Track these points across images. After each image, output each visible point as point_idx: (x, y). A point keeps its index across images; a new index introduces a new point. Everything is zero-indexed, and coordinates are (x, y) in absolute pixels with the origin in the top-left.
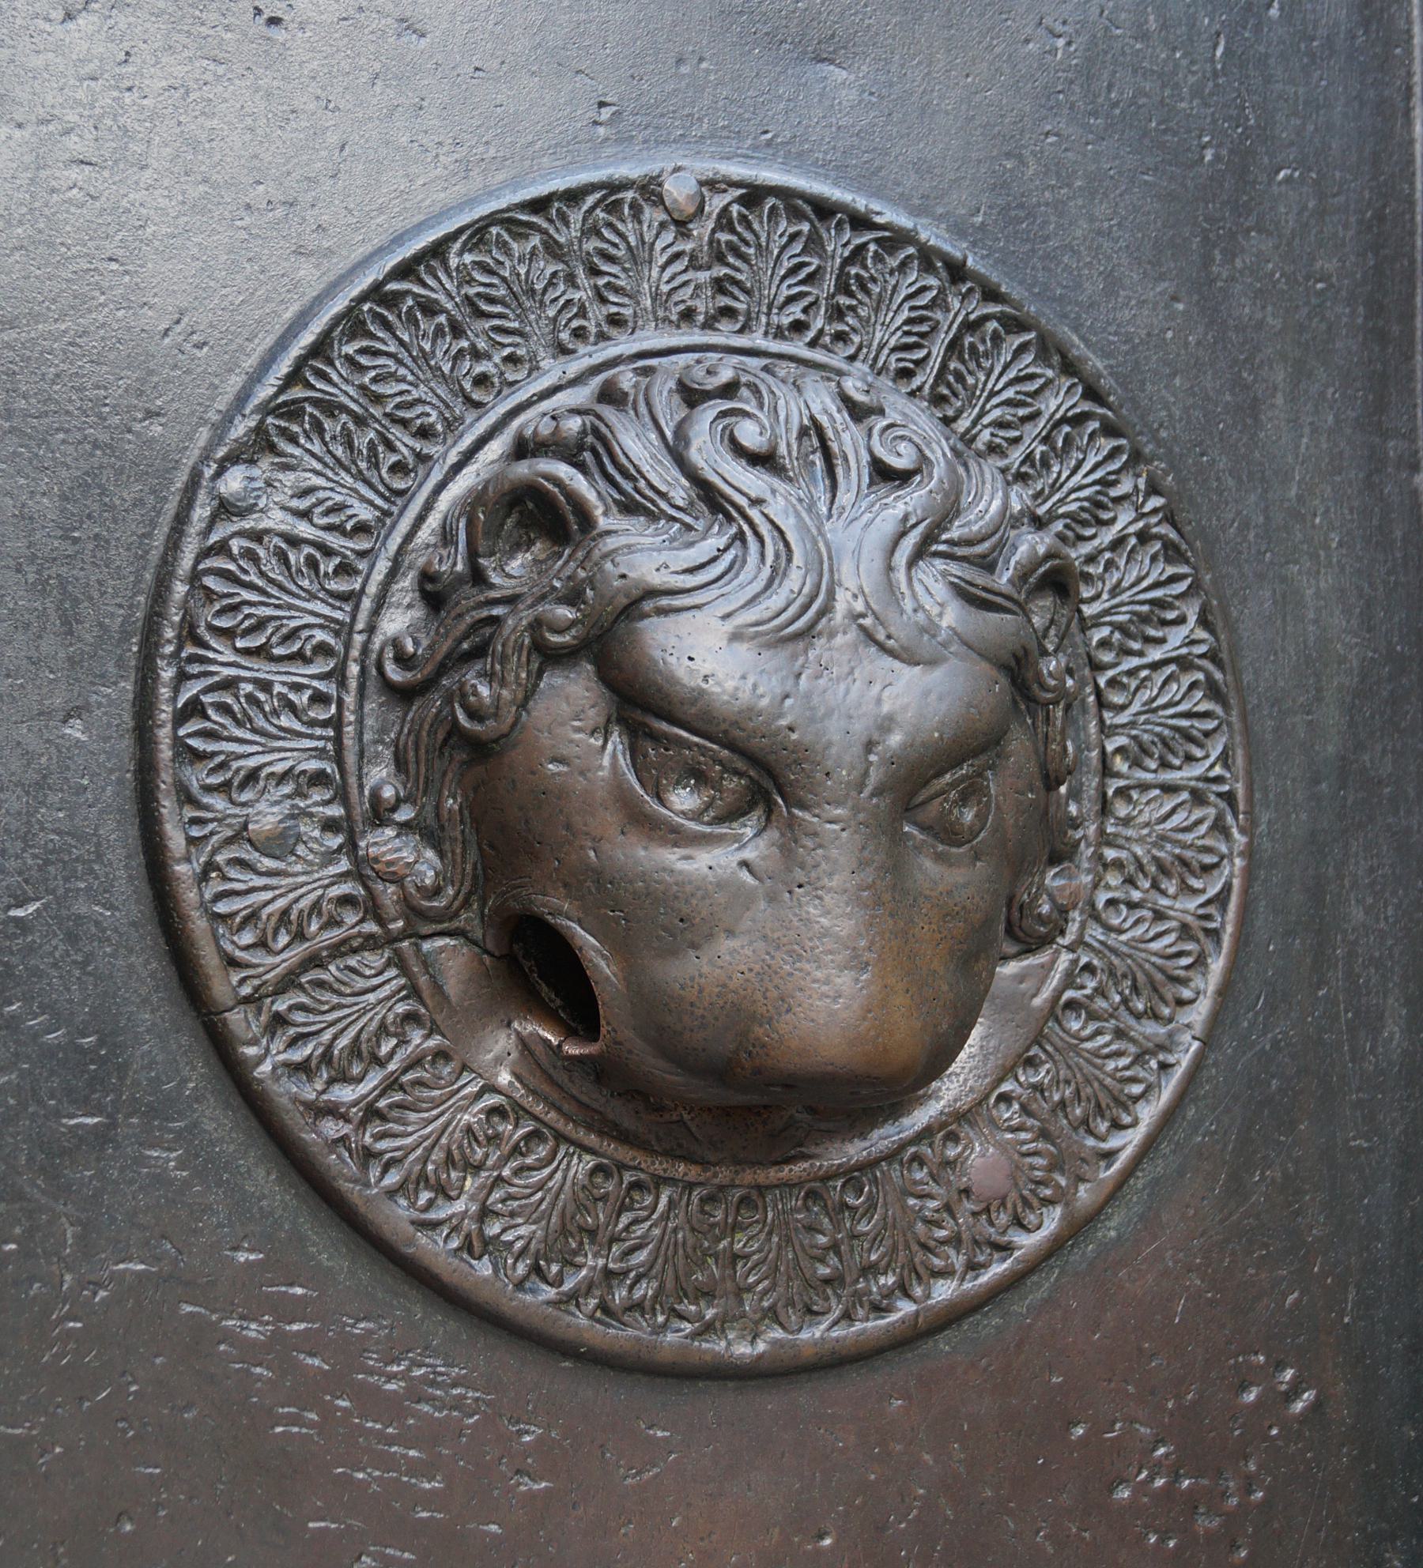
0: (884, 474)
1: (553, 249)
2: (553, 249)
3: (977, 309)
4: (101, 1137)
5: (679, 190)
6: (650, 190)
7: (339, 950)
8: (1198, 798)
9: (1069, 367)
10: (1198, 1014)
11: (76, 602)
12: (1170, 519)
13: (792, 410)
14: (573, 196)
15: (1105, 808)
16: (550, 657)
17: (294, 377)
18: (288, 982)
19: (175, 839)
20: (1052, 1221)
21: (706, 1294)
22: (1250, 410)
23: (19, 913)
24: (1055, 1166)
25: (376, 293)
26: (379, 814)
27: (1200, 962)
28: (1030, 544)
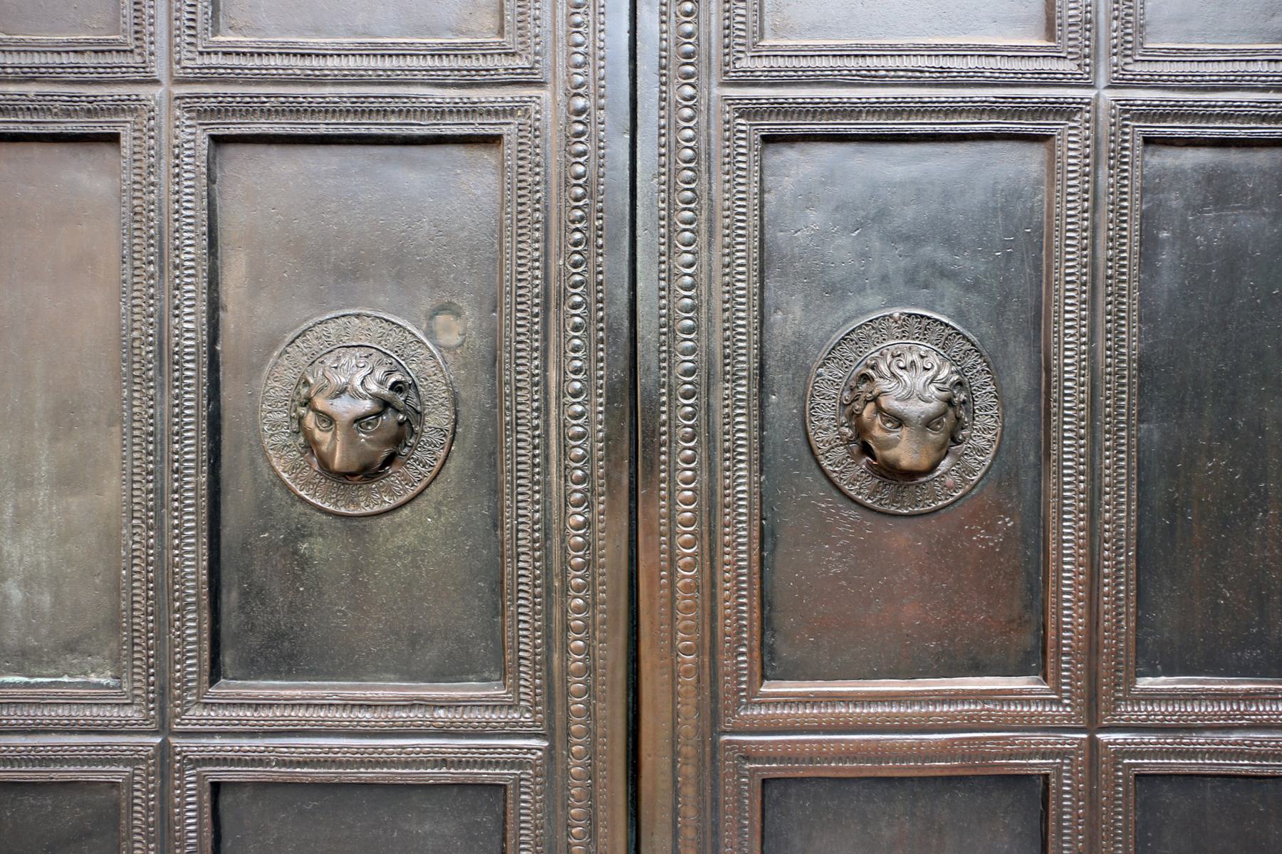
0: (925, 369)
1: (873, 328)
2: (873, 328)
3: (951, 332)
5: (896, 315)
6: (891, 316)
7: (836, 446)
8: (992, 417)
9: (968, 340)
10: (990, 456)
12: (988, 366)
13: (910, 359)
14: (877, 319)
17: (830, 353)
18: (828, 451)
19: (810, 429)
20: (961, 492)
21: (897, 502)
22: (1006, 344)
25: (843, 339)
26: (842, 425)
27: (991, 446)
28: (956, 377)
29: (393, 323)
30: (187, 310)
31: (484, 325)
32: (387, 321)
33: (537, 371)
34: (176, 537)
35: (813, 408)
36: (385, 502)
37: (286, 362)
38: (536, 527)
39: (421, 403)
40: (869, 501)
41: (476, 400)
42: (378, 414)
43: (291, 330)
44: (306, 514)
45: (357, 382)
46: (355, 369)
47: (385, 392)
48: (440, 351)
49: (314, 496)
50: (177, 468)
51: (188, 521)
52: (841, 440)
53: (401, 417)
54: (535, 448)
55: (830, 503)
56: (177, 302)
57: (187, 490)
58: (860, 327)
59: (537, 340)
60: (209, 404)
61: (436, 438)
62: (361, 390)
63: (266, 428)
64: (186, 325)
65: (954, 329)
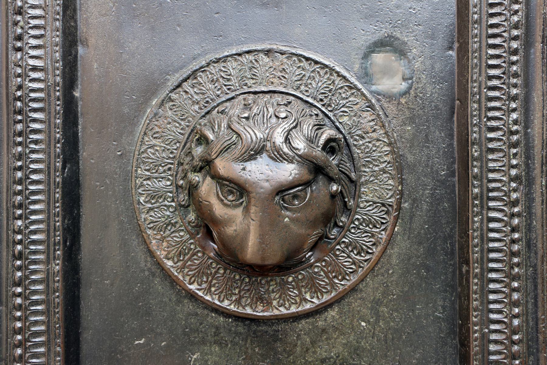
29: (316, 62)
30: (33, 42)
31: (438, 66)
32: (307, 59)
33: (515, 128)
34: (20, 344)
36: (306, 300)
37: (170, 113)
38: (516, 337)
39: (356, 169)
41: (427, 166)
42: (307, 184)
43: (176, 71)
44: (197, 314)
45: (279, 139)
46: (274, 120)
47: (318, 152)
48: (379, 100)
49: (208, 291)
50: (20, 253)
51: (36, 323)
53: (335, 188)
54: (513, 230)
56: (19, 31)
57: (35, 282)
59: (515, 86)
60: (64, 168)
61: (376, 213)
62: (286, 150)
63: (142, 199)
64: (32, 62)
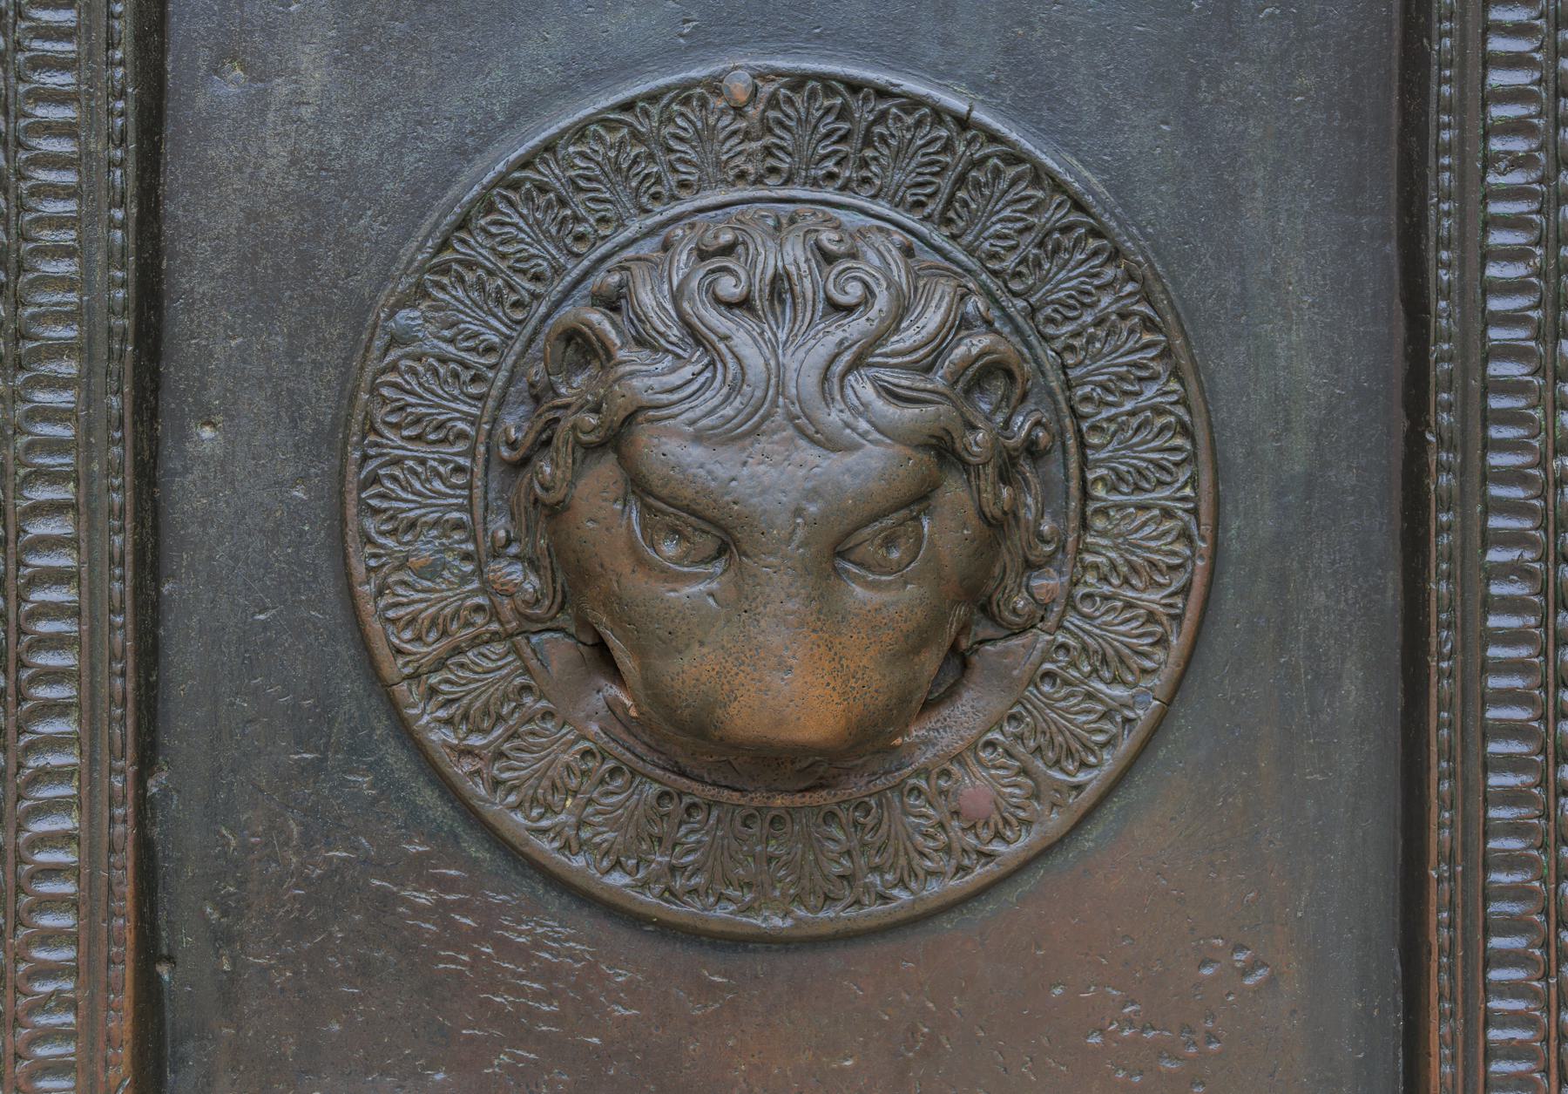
0: (835, 307)
2: (636, 136)
4: (318, 766)
5: (739, 85)
6: (714, 86)
7: (475, 642)
8: (1168, 514)
9: (1058, 186)
10: (1159, 682)
11: (300, 406)
12: (1148, 299)
14: (653, 97)
15: (1085, 525)
16: (590, 449)
17: (445, 245)
18: (440, 664)
19: (359, 570)
23: (262, 617)
24: (1036, 795)
25: (504, 181)
27: (1162, 642)
35: (375, 479)
40: (617, 879)
52: (495, 614)
55: (447, 884)
58: (579, 132)
65: (994, 138)
